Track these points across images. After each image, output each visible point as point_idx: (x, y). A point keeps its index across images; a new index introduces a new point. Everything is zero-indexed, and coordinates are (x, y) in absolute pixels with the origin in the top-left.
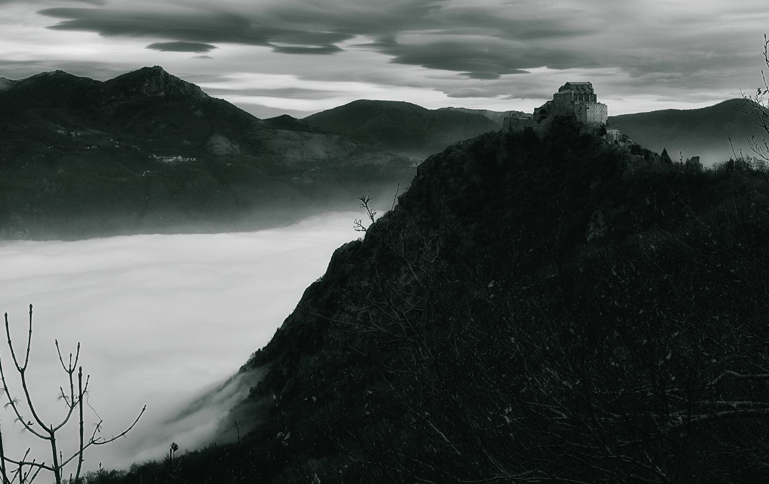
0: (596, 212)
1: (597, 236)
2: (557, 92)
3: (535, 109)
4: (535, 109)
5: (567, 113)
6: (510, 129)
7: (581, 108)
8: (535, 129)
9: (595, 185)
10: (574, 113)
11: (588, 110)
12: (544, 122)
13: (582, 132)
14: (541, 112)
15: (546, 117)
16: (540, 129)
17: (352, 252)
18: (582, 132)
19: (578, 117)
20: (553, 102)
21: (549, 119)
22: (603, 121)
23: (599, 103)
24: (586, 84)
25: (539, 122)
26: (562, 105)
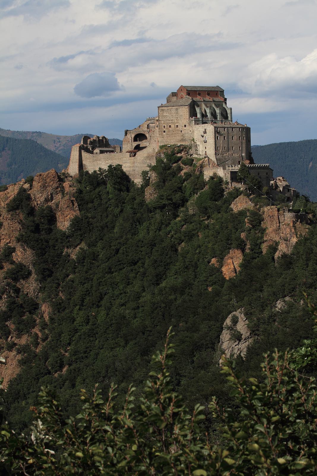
0: (234, 313)
1: (235, 356)
5: (182, 140)
6: (81, 166)
7: (205, 132)
8: (126, 168)
9: (232, 267)
10: (193, 140)
11: (217, 135)
13: (208, 174)
16: (136, 166)
18: (208, 174)
19: (201, 149)
21: (152, 146)
24: (213, 89)
26: (173, 126)
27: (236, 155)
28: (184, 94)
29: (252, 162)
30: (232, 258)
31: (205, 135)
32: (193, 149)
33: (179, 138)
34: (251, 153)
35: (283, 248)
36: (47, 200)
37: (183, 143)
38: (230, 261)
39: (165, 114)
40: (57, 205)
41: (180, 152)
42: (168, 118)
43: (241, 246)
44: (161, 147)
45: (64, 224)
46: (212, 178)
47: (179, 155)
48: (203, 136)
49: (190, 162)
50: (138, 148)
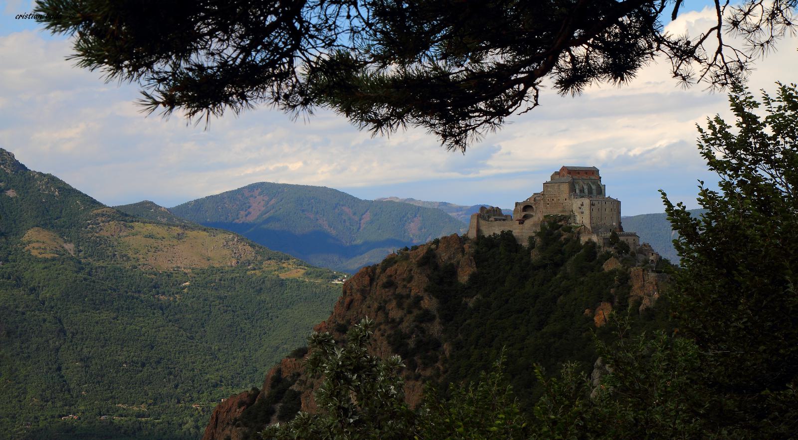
2: (549, 180)
3: (517, 204)
4: (517, 204)
5: (563, 211)
6: (479, 231)
7: (582, 205)
8: (516, 232)
9: (603, 317)
11: (592, 207)
12: (528, 223)
13: (584, 239)
14: (526, 208)
15: (532, 216)
16: (524, 232)
17: (243, 408)
18: (584, 239)
19: (578, 218)
20: (543, 194)
21: (538, 216)
22: (614, 224)
23: (609, 197)
25: (521, 222)
26: (555, 200)
27: (608, 224)
28: (565, 173)
29: (621, 229)
30: (603, 310)
31: (582, 207)
32: (572, 218)
33: (560, 209)
34: (621, 223)
35: (646, 302)
36: (450, 258)
37: (564, 214)
38: (601, 312)
39: (549, 190)
40: (458, 263)
41: (560, 221)
42: (552, 193)
43: (610, 300)
44: (545, 217)
45: (464, 278)
46: (587, 243)
47: (560, 223)
48: (580, 208)
49: (569, 229)
50: (526, 217)
